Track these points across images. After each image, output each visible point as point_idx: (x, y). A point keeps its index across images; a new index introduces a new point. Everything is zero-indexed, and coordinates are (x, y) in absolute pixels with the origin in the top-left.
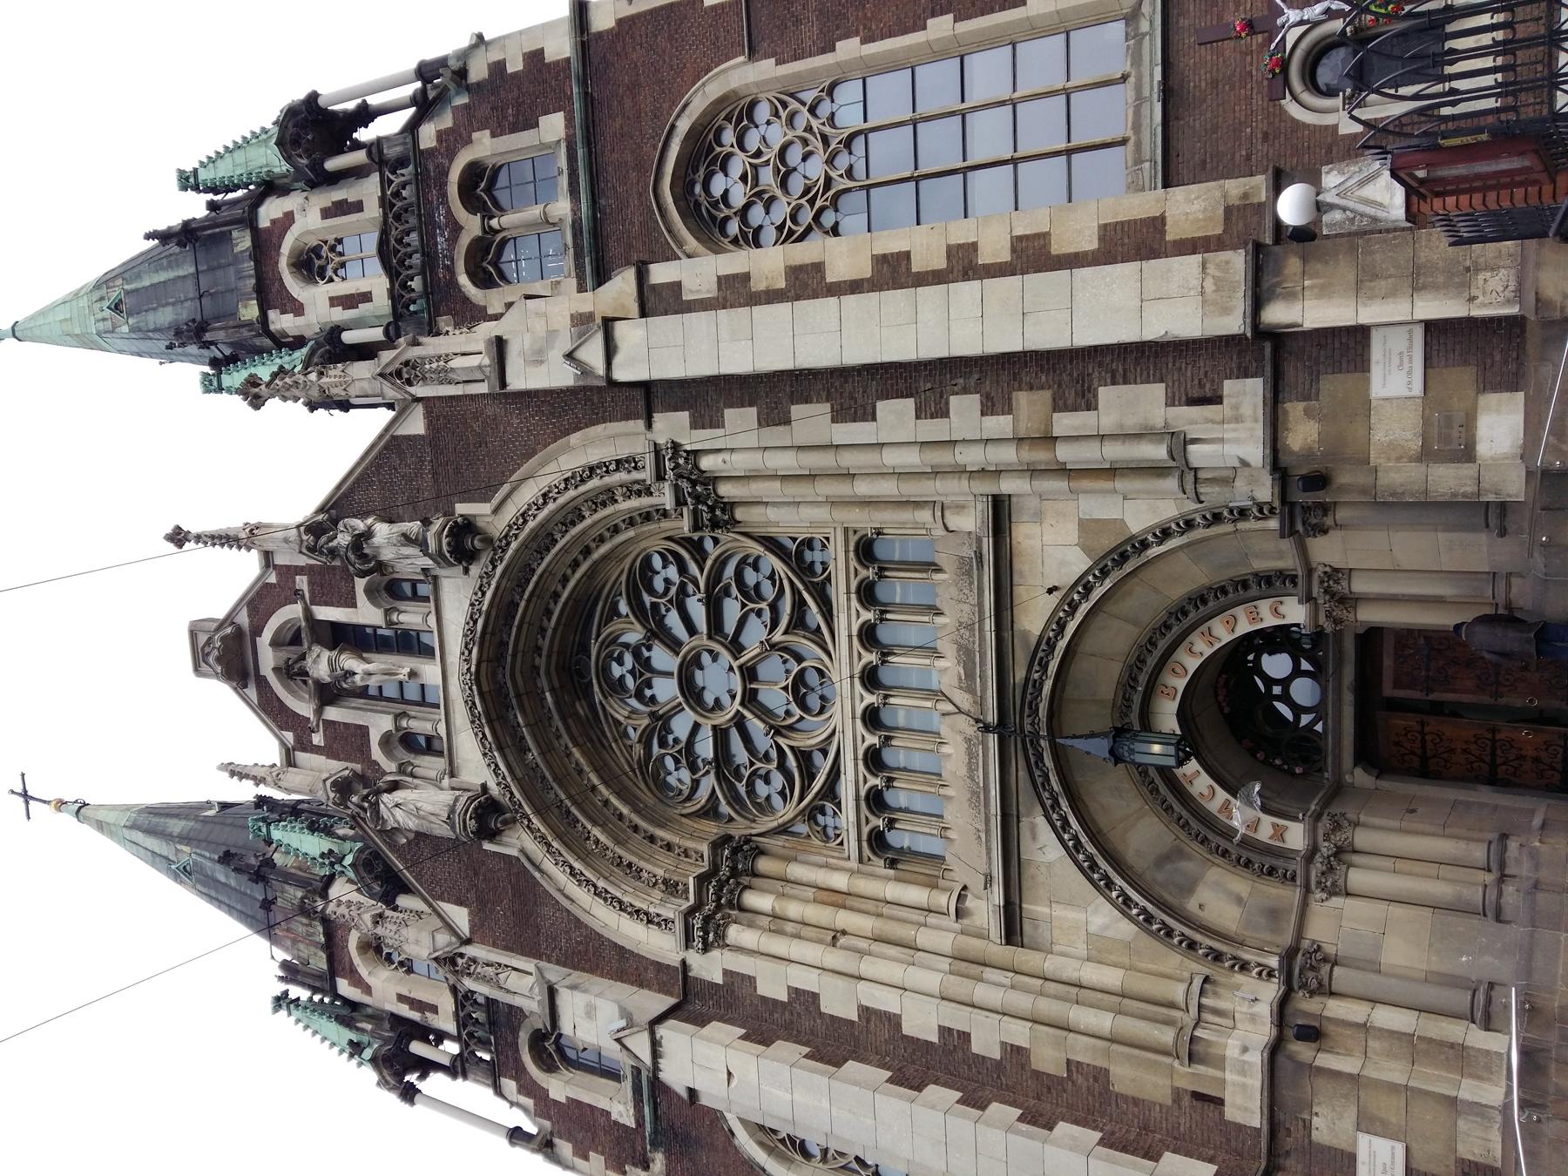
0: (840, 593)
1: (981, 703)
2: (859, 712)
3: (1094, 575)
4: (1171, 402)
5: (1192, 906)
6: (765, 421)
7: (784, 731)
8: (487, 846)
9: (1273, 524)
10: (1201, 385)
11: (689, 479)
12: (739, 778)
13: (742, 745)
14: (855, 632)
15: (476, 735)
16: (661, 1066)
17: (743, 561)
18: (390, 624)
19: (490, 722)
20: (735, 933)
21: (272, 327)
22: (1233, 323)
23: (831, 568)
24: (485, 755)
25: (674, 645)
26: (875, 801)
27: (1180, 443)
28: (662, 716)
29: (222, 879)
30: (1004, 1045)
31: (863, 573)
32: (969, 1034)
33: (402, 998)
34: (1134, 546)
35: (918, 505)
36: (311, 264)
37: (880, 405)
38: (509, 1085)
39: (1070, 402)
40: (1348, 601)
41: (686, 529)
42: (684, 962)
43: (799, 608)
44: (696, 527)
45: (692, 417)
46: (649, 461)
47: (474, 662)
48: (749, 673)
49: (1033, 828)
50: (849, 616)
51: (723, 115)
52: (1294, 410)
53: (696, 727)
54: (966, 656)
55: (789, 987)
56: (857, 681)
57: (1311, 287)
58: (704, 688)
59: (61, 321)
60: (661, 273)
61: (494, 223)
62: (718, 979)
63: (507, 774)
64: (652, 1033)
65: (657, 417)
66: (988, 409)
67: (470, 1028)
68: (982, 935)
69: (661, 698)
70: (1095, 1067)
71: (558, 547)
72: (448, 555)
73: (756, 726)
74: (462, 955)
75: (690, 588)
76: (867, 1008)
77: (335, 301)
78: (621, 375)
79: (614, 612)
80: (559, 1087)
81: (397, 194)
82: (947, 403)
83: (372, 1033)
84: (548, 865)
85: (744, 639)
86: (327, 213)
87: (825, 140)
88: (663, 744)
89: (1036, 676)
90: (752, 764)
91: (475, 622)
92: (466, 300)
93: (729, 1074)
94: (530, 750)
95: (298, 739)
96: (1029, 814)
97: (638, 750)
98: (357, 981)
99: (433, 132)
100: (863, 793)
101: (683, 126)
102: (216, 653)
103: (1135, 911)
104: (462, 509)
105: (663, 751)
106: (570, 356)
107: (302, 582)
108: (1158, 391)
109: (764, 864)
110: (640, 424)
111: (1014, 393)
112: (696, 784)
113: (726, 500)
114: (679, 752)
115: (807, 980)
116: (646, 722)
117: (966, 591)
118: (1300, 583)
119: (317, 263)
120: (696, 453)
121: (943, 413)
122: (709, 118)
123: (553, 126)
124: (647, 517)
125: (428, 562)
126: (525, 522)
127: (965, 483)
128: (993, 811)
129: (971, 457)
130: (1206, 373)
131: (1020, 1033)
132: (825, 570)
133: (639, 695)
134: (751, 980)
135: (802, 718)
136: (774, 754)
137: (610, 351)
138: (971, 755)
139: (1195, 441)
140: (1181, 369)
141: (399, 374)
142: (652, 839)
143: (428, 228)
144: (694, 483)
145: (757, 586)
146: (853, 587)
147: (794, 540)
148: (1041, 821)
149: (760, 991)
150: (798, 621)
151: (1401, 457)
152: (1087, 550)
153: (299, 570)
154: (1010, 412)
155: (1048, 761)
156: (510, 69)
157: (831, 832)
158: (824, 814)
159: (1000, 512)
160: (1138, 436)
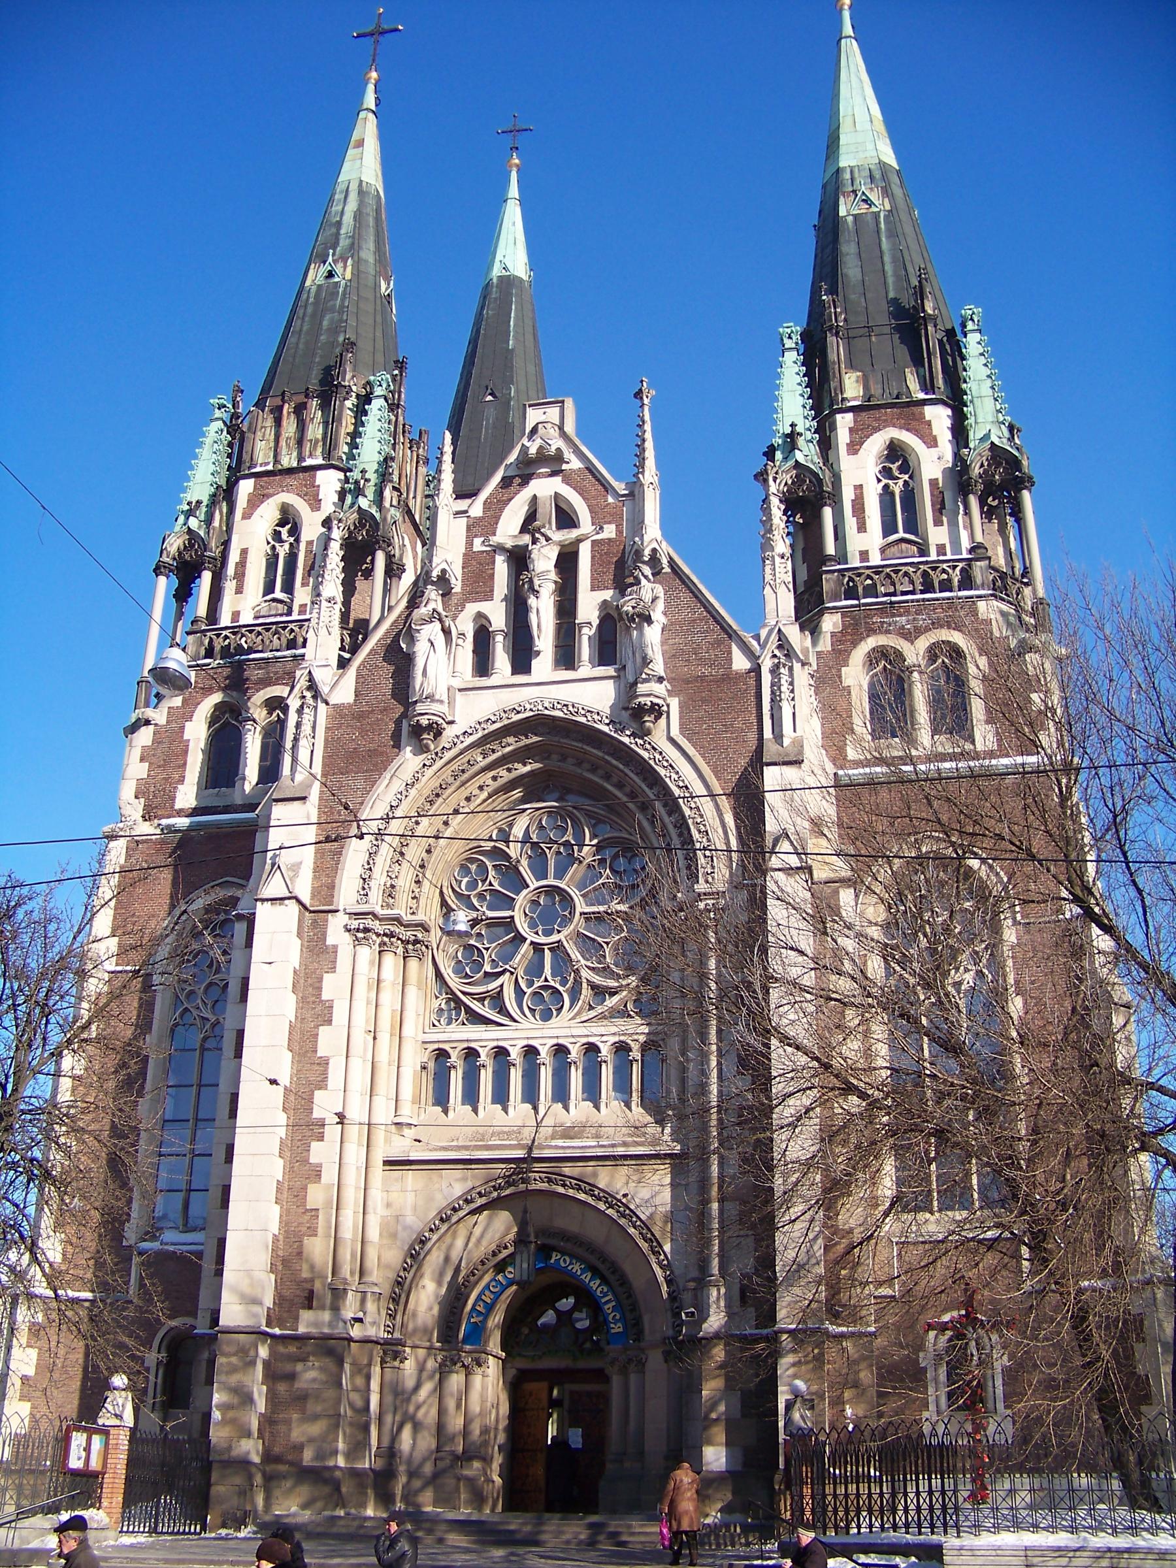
20: (366, 954)
21: (838, 417)
29: (325, 323)
30: (320, 1165)
33: (244, 552)
40: (624, 1371)
62: (330, 941)
63: (465, 744)
77: (859, 488)
86: (933, 483)
92: (855, 644)
96: (474, 1177)
98: (255, 501)
104: (674, 703)
107: (610, 532)
115: (340, 1014)
119: (894, 467)
131: (329, 1175)
134: (333, 969)
137: (789, 870)
148: (469, 1184)
149: (325, 975)
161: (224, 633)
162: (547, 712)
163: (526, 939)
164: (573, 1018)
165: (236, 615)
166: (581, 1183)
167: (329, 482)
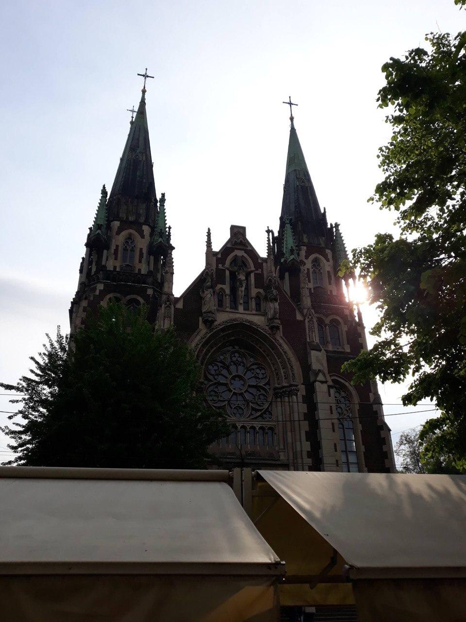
8: (200, 319)
14: (254, 425)
18: (251, 299)
33: (117, 246)
35: (284, 446)
36: (316, 262)
37: (309, 443)
44: (275, 389)
48: (241, 394)
50: (257, 424)
53: (227, 378)
58: (235, 380)
60: (332, 391)
74: (170, 304)
75: (257, 380)
79: (252, 357)
84: (198, 338)
86: (329, 272)
88: (221, 366)
107: (259, 271)
114: (220, 372)
120: (297, 395)
124: (277, 374)
135: (231, 408)
137: (322, 382)
144: (289, 392)
150: (253, 409)
164: (248, 418)
165: (115, 267)
167: (146, 229)
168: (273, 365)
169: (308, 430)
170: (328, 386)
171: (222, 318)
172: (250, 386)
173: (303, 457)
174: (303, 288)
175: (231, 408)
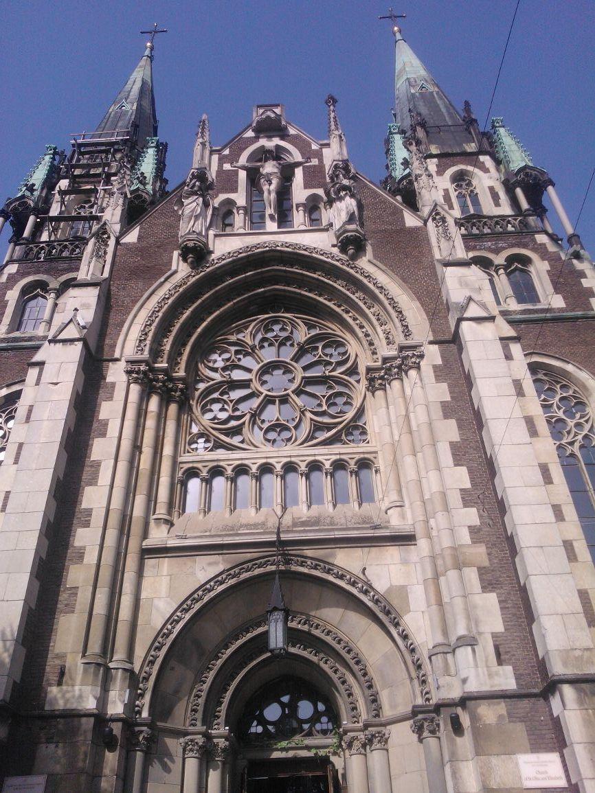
0: (336, 451)
1: (288, 532)
2: (270, 461)
3: (374, 596)
4: (495, 636)
5: (173, 663)
6: (444, 405)
7: (253, 419)
8: (176, 254)
9: (420, 701)
10: (507, 653)
11: (401, 365)
12: (221, 394)
13: (242, 395)
15: (241, 249)
16: (58, 345)
17: (349, 397)
19: (249, 256)
22: (558, 668)
23: (352, 445)
24: (229, 253)
25: (296, 358)
26: (217, 471)
27: (470, 641)
28: (254, 352)
29: (120, 124)
30: (84, 548)
31: (352, 462)
32: (89, 527)
34: (395, 618)
35: (400, 492)
38: (13, 269)
39: (484, 577)
41: (368, 364)
42: (117, 360)
43: (327, 428)
44: (369, 370)
45: (440, 365)
46: (409, 342)
47: (282, 249)
48: (284, 400)
49: (216, 563)
50: (327, 455)
51: (577, 389)
52: (501, 708)
53: (249, 370)
54: (315, 522)
55: (108, 420)
56: (288, 459)
57: (588, 715)
59: (411, 62)
60: (516, 349)
61: (502, 271)
62: (109, 379)
63: (219, 264)
64: (78, 340)
65: (436, 347)
66: (473, 530)
67: (47, 248)
68: (145, 535)
69: (263, 351)
70: (75, 604)
71: (351, 295)
72: (345, 235)
73: (255, 403)
74: (109, 237)
76: (100, 466)
78: (465, 325)
80: (12, 296)
81: (509, 222)
82: (472, 506)
83: (40, 196)
84: (168, 286)
85: (303, 396)
87: (571, 444)
88: (237, 352)
89: (309, 563)
90: (231, 401)
91: (305, 250)
93: (56, 384)
94: (232, 278)
95: (226, 156)
97: (233, 338)
99: (544, 242)
100: (221, 464)
101: (570, 368)
102: (273, 115)
103: (169, 627)
105: (233, 353)
106: (470, 299)
107: (315, 162)
108: (499, 627)
109: (173, 408)
110: (431, 338)
111: (483, 545)
112: (215, 370)
113: (387, 386)
116: (250, 343)
117: (353, 521)
118: (374, 719)
119: (464, 184)
120: (418, 368)
121: (466, 504)
122: (575, 382)
123: (558, 302)
125: (337, 225)
126: (366, 277)
127: (421, 518)
128: (226, 539)
129: (439, 521)
130: (514, 655)
131: (91, 558)
132: (350, 441)
133: (264, 340)
134: (110, 398)
136: (238, 413)
138: (255, 526)
139: (474, 651)
140: (514, 640)
141: (438, 214)
142: (184, 345)
143: (495, 236)
144: (399, 367)
145: (335, 404)
146: (343, 457)
147: (365, 424)
148: (221, 568)
151: (484, 776)
152: (390, 590)
153: (321, 160)
154: (473, 543)
155: (257, 571)
156: (583, 281)
157: (194, 446)
158: (205, 442)
159: (406, 539)
160: (468, 617)
161: (42, 245)
162: (278, 248)
163: (262, 393)
166: (318, 563)
168: (362, 327)
169: (459, 440)
170: (501, 339)
171: (224, 248)
172: (309, 381)
173: (451, 505)
174: (420, 176)
175: (261, 429)
